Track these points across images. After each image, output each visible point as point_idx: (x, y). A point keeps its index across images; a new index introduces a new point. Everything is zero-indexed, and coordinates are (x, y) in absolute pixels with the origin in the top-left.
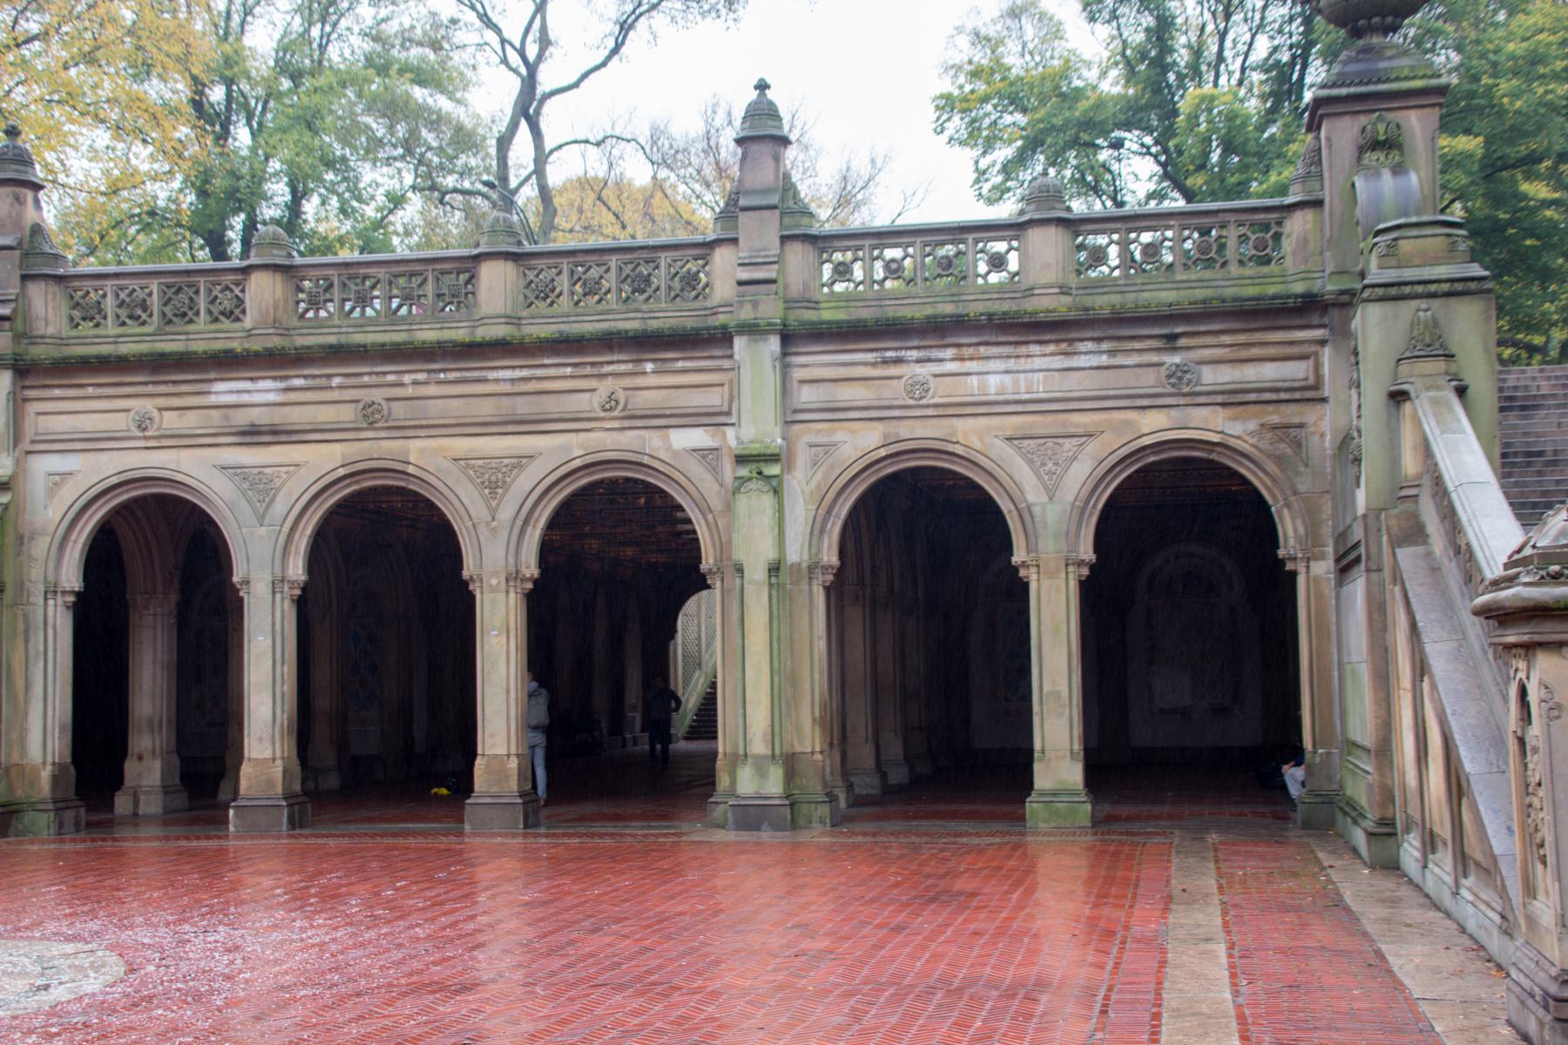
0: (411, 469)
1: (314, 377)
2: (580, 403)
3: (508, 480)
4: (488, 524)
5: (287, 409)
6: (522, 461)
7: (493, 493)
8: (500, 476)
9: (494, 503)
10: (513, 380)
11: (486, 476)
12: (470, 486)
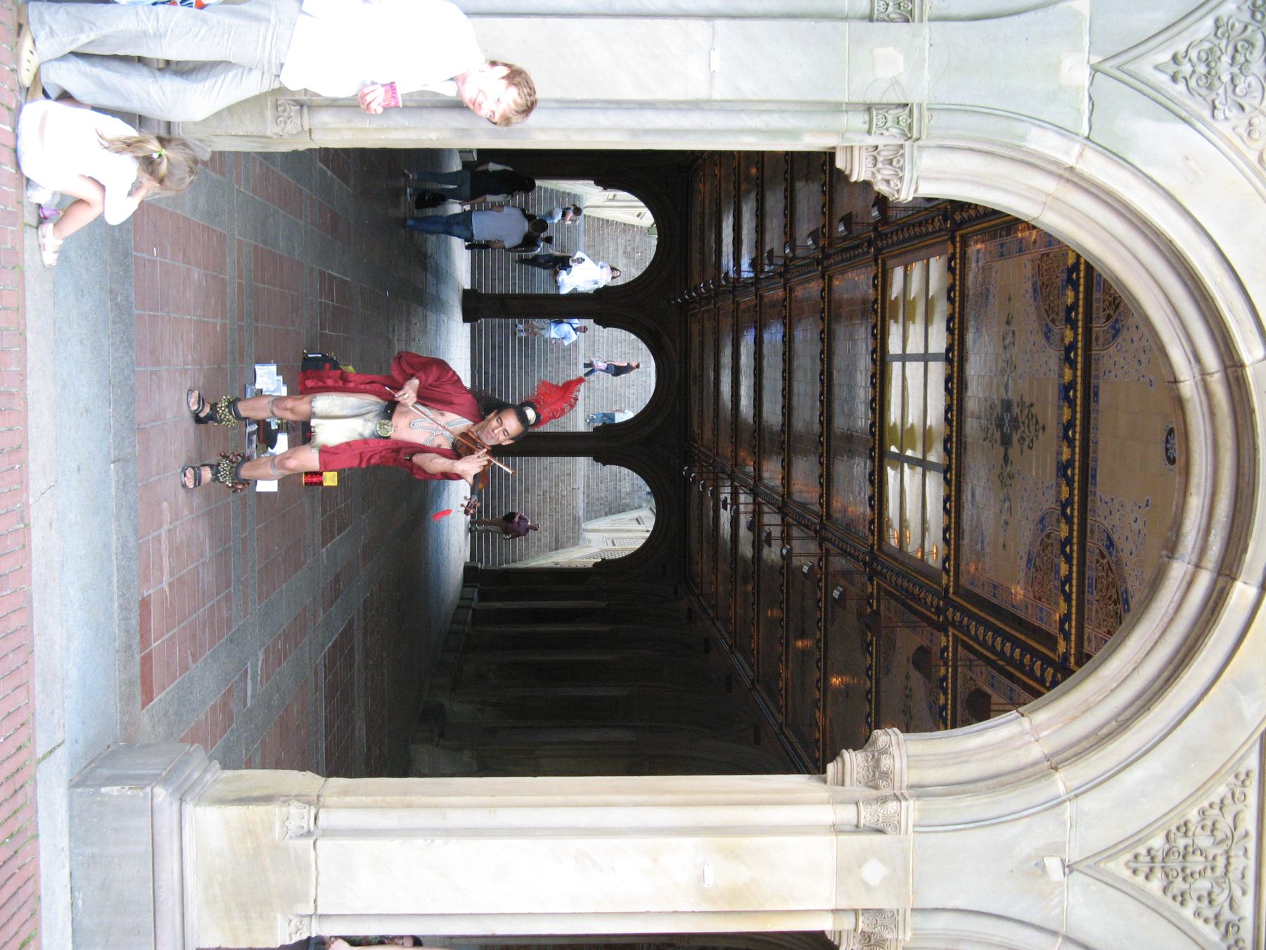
3: (1188, 912)
4: (1056, 849)
7: (1151, 864)
8: (1203, 885)
9: (1119, 867)
11: (1204, 841)
12: (1177, 793)
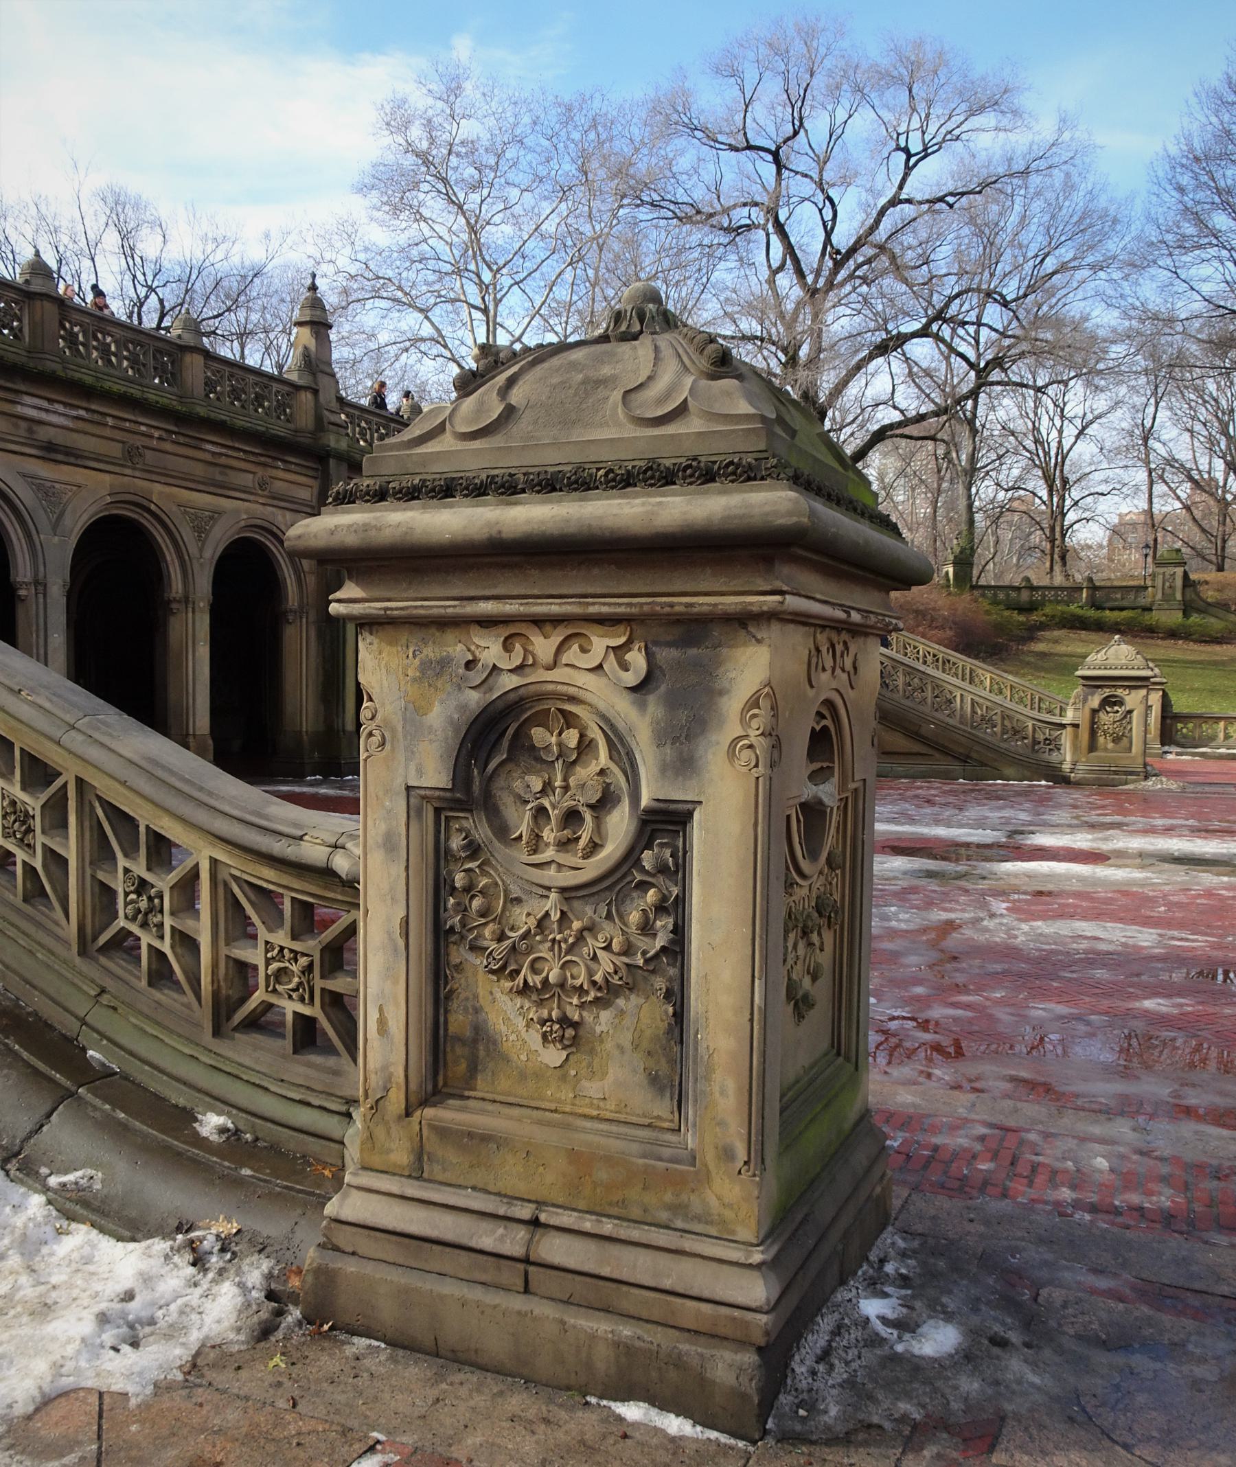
0: (153, 507)
1: (94, 411)
2: (247, 480)
5: (75, 435)
6: (216, 514)
10: (214, 453)
